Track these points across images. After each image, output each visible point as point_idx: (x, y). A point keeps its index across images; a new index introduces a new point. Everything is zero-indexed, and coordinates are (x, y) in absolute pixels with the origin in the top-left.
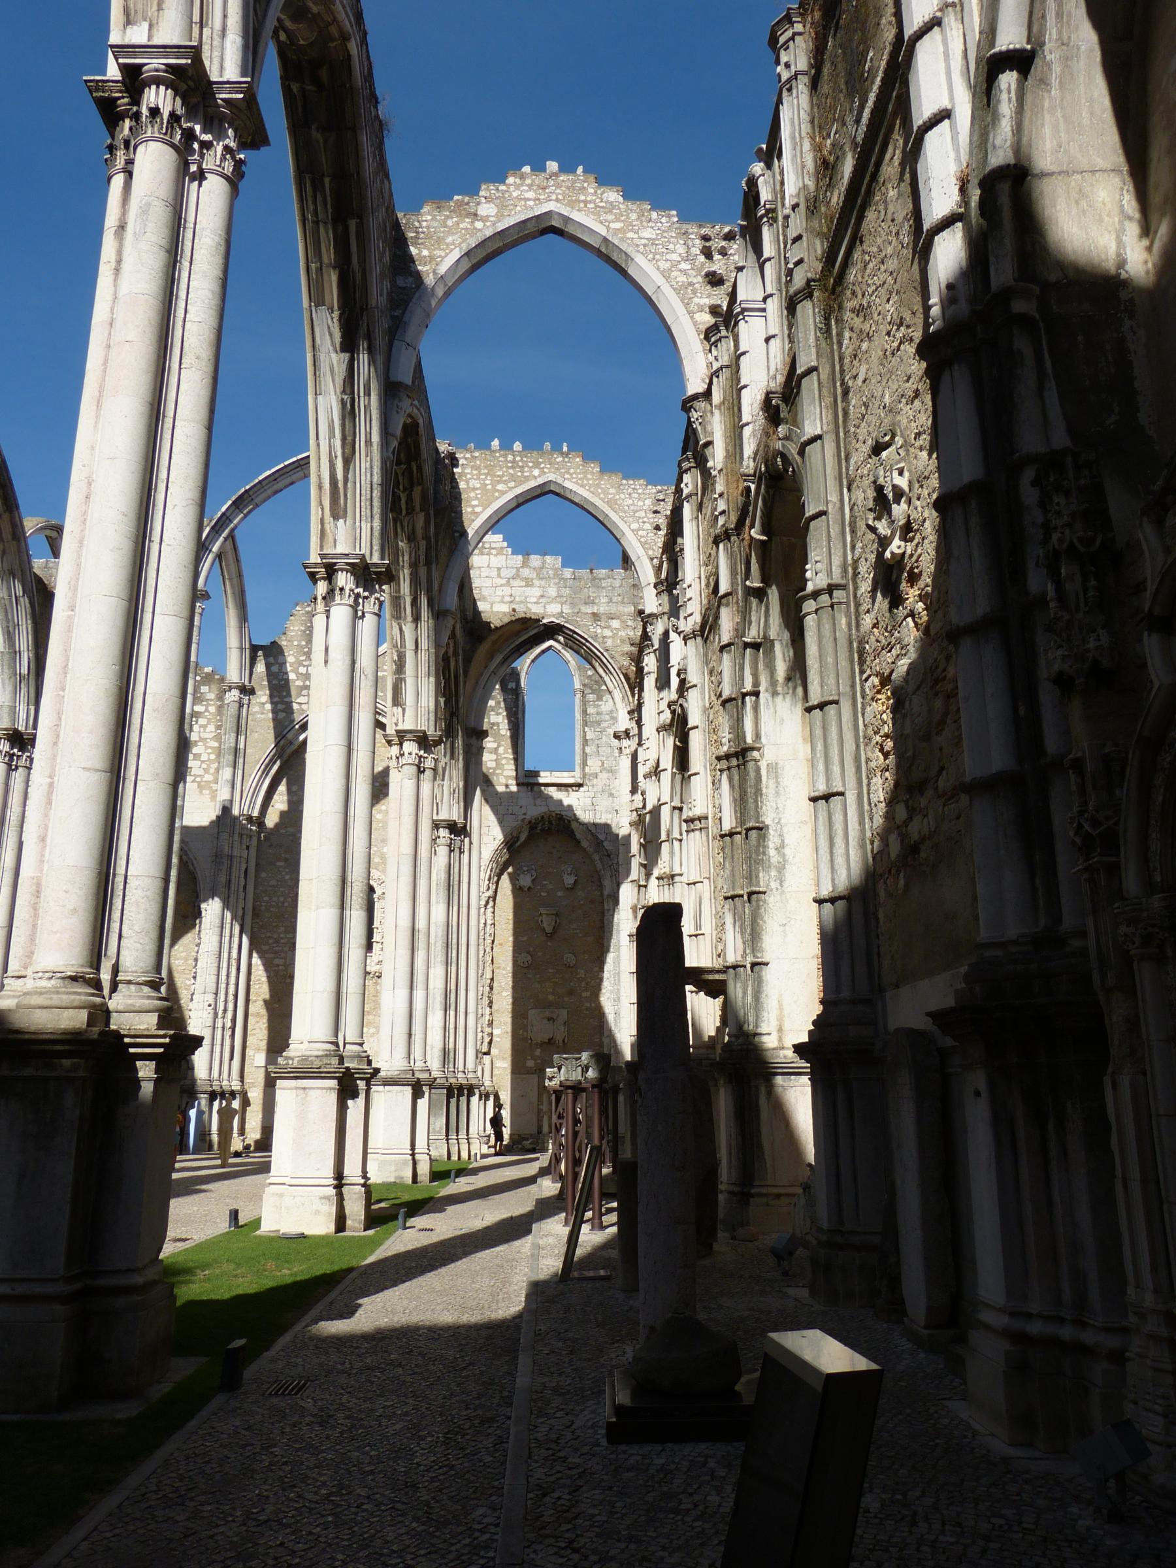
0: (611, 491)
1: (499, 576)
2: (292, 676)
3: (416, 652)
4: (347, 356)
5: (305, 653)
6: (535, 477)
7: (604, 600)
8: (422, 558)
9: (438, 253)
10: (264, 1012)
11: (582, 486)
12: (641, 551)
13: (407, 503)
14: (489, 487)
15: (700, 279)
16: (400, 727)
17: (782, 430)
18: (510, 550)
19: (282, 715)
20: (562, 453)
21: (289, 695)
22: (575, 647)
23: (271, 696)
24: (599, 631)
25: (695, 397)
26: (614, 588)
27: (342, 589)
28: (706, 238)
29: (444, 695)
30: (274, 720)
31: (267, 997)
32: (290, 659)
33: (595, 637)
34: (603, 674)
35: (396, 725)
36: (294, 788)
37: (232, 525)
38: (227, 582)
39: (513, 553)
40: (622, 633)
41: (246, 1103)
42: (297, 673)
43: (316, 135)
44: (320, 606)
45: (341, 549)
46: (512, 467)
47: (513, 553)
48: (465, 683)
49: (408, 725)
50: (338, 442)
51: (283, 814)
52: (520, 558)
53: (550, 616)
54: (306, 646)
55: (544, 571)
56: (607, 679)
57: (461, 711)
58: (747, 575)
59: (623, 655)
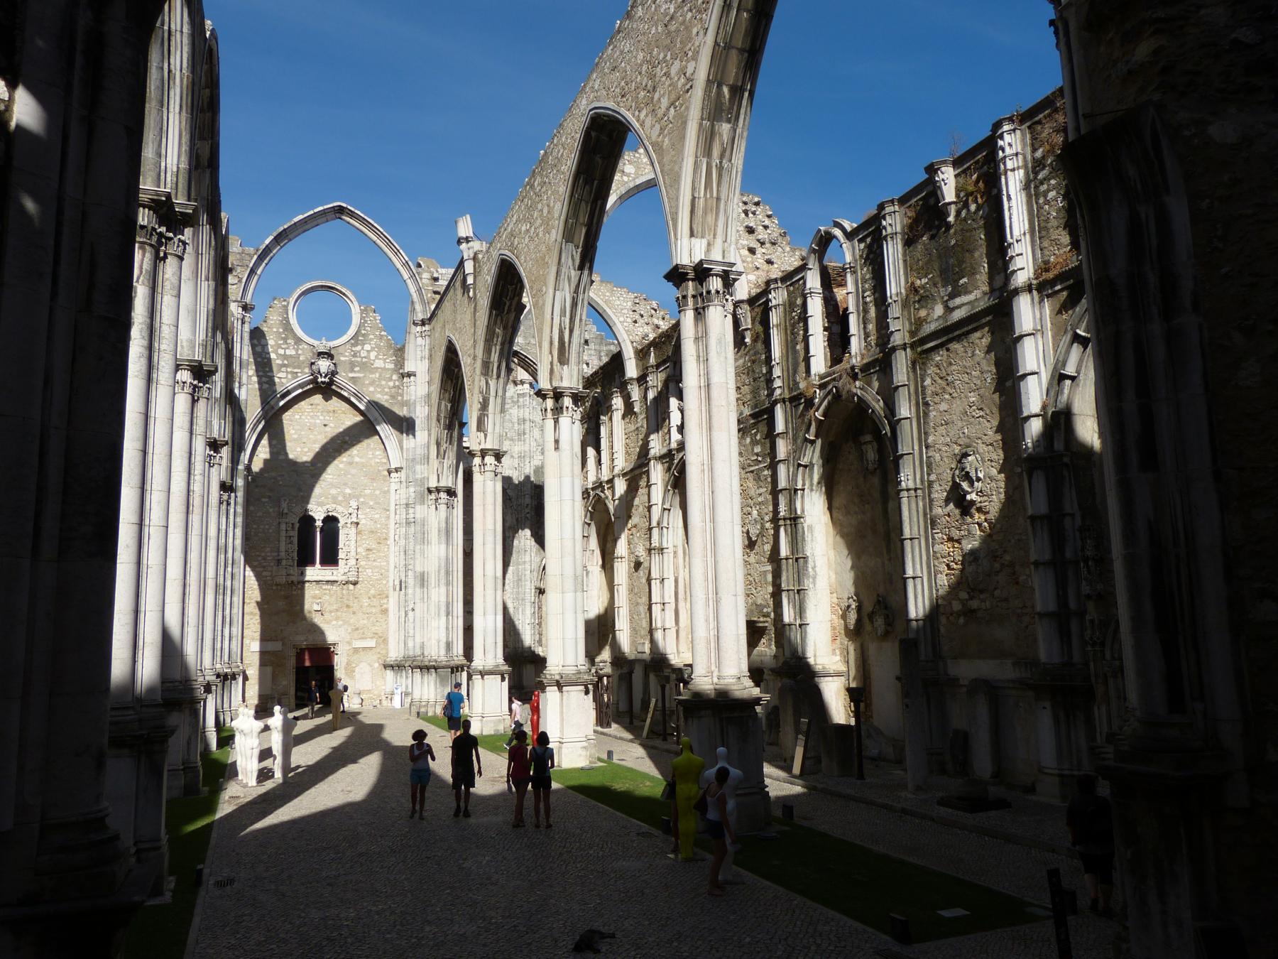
2: (273, 356)
10: (257, 611)
12: (625, 337)
16: (483, 446)
17: (857, 383)
19: (265, 386)
21: (271, 370)
23: (257, 371)
25: (742, 302)
28: (745, 203)
30: (260, 389)
31: (259, 599)
32: (271, 342)
36: (274, 442)
41: (246, 678)
42: (277, 353)
43: (598, 159)
45: (565, 384)
49: (488, 446)
50: (567, 321)
51: (266, 461)
58: (808, 431)
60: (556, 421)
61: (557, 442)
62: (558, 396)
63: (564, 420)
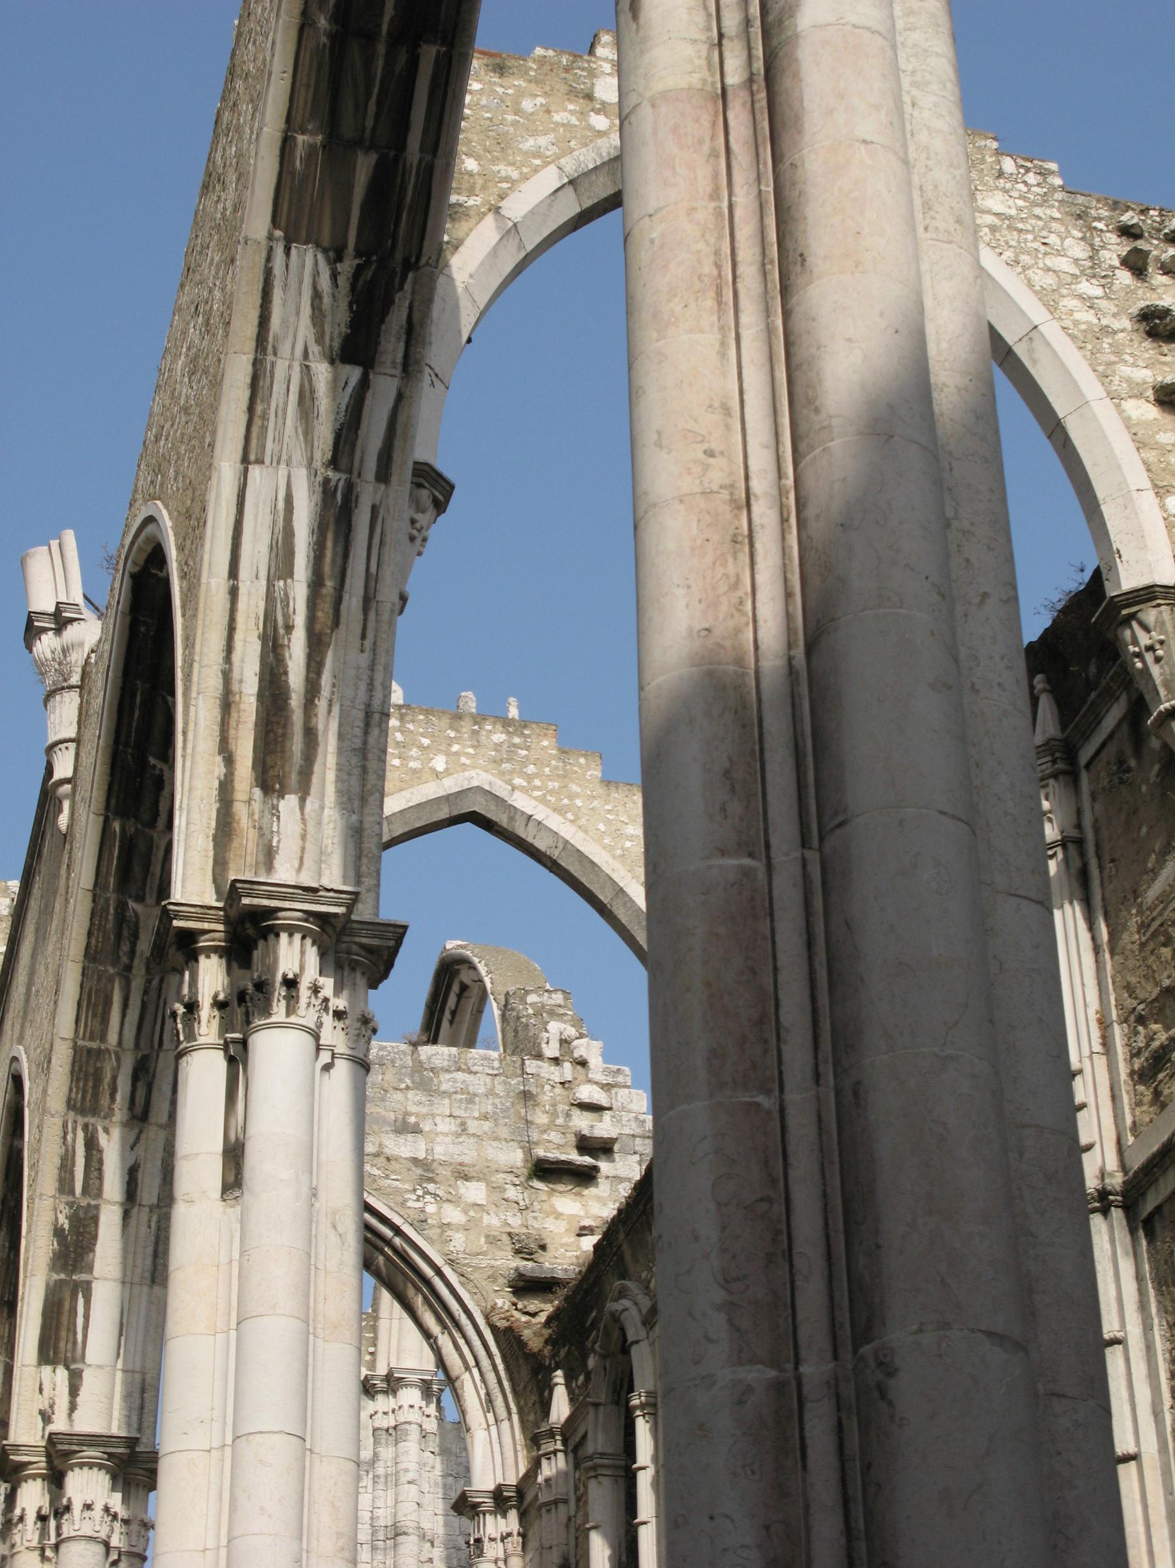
3: (126, 1215)
4: (354, 374)
6: (437, 775)
9: (504, 169)
11: (560, 810)
15: (1126, 323)
16: (60, 1424)
20: (506, 723)
24: (431, 1209)
26: (471, 1099)
27: (291, 984)
33: (421, 1223)
34: (435, 1328)
35: (46, 1417)
40: (493, 1221)
44: (208, 1027)
50: (299, 590)
56: (444, 1341)
59: (493, 1278)
60: (237, 1057)
61: (234, 1155)
62: (248, 930)
63: (278, 1048)
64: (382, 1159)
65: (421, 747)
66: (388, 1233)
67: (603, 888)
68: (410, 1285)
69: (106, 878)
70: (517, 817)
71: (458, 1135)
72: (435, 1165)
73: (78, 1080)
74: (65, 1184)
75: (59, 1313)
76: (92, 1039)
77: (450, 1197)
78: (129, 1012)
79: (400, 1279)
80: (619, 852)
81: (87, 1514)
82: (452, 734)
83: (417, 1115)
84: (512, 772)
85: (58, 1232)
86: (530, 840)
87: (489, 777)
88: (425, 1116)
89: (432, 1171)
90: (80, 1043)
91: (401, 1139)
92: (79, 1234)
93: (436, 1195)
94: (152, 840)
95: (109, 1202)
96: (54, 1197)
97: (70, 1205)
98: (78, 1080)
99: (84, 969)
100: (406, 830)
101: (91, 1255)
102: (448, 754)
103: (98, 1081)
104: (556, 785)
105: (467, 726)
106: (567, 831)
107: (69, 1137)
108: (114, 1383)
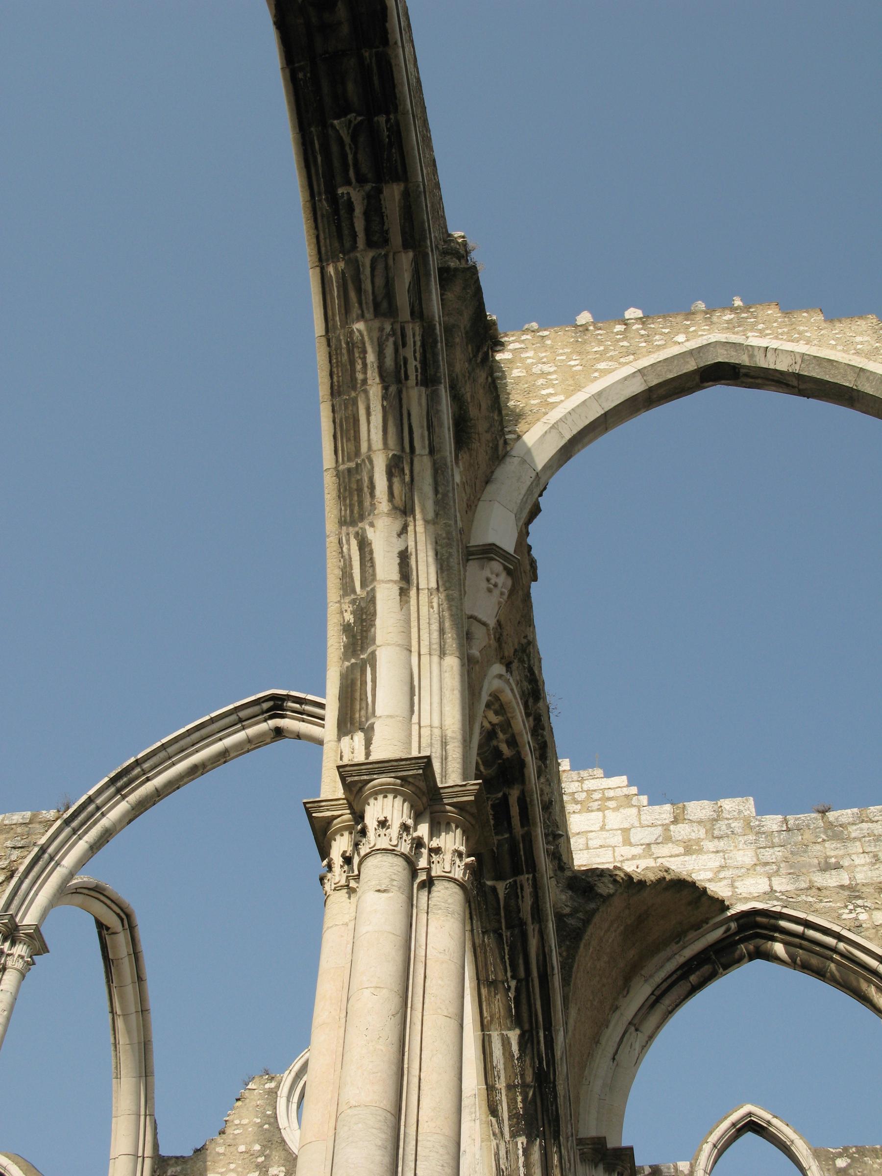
0: (859, 339)
1: (627, 842)
3: (404, 592)
5: (258, 1166)
7: (860, 860)
8: (413, 365)
13: (366, 214)
14: (579, 368)
18: (644, 799)
20: (733, 309)
22: (814, 961)
24: (863, 917)
29: (517, 1021)
33: (858, 927)
37: (105, 822)
38: (120, 1023)
39: (651, 803)
46: (625, 338)
47: (651, 803)
48: (566, 980)
52: (665, 811)
53: (747, 900)
54: (261, 1153)
55: (722, 825)
57: (562, 1069)
64: (814, 891)
65: (662, 334)
66: (831, 941)
67: (844, 376)
68: (862, 981)
69: (333, 319)
70: (756, 353)
71: (874, 864)
72: (859, 887)
73: (345, 499)
74: (347, 586)
75: (353, 691)
76: (349, 460)
77: (877, 906)
78: (373, 418)
79: (852, 978)
80: (853, 351)
81: (382, 831)
82: (688, 323)
83: (836, 857)
84: (744, 331)
85: (347, 628)
86: (772, 367)
87: (725, 335)
88: (842, 857)
89: (858, 891)
90: (341, 467)
91: (827, 875)
92: (362, 620)
93: (864, 907)
94: (357, 261)
95: (383, 581)
96: (339, 602)
97: (353, 602)
98: (345, 499)
99: (333, 406)
100: (661, 380)
101: (373, 630)
102: (686, 332)
103: (360, 490)
104: (786, 330)
105: (699, 317)
106: (801, 348)
107: (345, 549)
108: (410, 735)
